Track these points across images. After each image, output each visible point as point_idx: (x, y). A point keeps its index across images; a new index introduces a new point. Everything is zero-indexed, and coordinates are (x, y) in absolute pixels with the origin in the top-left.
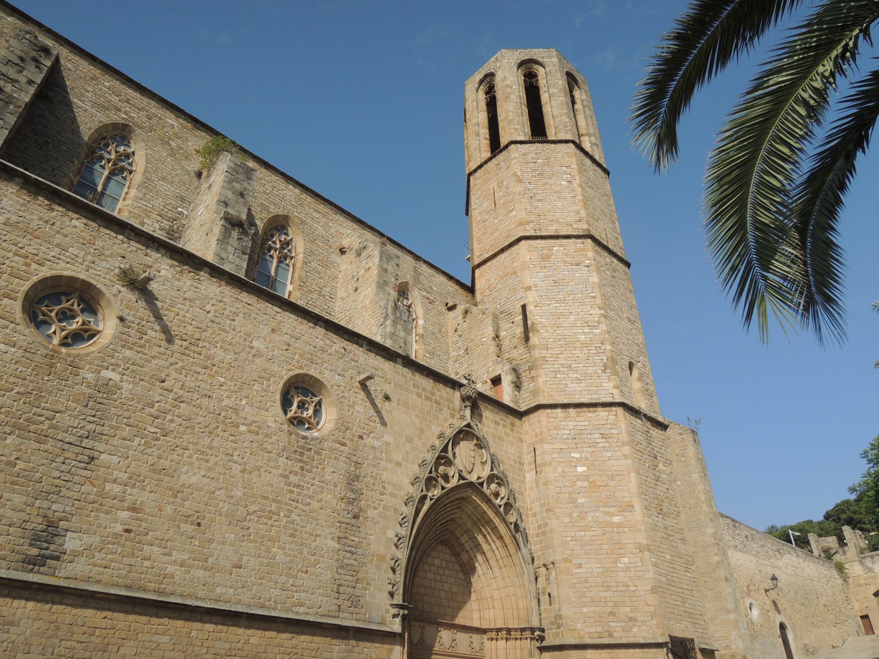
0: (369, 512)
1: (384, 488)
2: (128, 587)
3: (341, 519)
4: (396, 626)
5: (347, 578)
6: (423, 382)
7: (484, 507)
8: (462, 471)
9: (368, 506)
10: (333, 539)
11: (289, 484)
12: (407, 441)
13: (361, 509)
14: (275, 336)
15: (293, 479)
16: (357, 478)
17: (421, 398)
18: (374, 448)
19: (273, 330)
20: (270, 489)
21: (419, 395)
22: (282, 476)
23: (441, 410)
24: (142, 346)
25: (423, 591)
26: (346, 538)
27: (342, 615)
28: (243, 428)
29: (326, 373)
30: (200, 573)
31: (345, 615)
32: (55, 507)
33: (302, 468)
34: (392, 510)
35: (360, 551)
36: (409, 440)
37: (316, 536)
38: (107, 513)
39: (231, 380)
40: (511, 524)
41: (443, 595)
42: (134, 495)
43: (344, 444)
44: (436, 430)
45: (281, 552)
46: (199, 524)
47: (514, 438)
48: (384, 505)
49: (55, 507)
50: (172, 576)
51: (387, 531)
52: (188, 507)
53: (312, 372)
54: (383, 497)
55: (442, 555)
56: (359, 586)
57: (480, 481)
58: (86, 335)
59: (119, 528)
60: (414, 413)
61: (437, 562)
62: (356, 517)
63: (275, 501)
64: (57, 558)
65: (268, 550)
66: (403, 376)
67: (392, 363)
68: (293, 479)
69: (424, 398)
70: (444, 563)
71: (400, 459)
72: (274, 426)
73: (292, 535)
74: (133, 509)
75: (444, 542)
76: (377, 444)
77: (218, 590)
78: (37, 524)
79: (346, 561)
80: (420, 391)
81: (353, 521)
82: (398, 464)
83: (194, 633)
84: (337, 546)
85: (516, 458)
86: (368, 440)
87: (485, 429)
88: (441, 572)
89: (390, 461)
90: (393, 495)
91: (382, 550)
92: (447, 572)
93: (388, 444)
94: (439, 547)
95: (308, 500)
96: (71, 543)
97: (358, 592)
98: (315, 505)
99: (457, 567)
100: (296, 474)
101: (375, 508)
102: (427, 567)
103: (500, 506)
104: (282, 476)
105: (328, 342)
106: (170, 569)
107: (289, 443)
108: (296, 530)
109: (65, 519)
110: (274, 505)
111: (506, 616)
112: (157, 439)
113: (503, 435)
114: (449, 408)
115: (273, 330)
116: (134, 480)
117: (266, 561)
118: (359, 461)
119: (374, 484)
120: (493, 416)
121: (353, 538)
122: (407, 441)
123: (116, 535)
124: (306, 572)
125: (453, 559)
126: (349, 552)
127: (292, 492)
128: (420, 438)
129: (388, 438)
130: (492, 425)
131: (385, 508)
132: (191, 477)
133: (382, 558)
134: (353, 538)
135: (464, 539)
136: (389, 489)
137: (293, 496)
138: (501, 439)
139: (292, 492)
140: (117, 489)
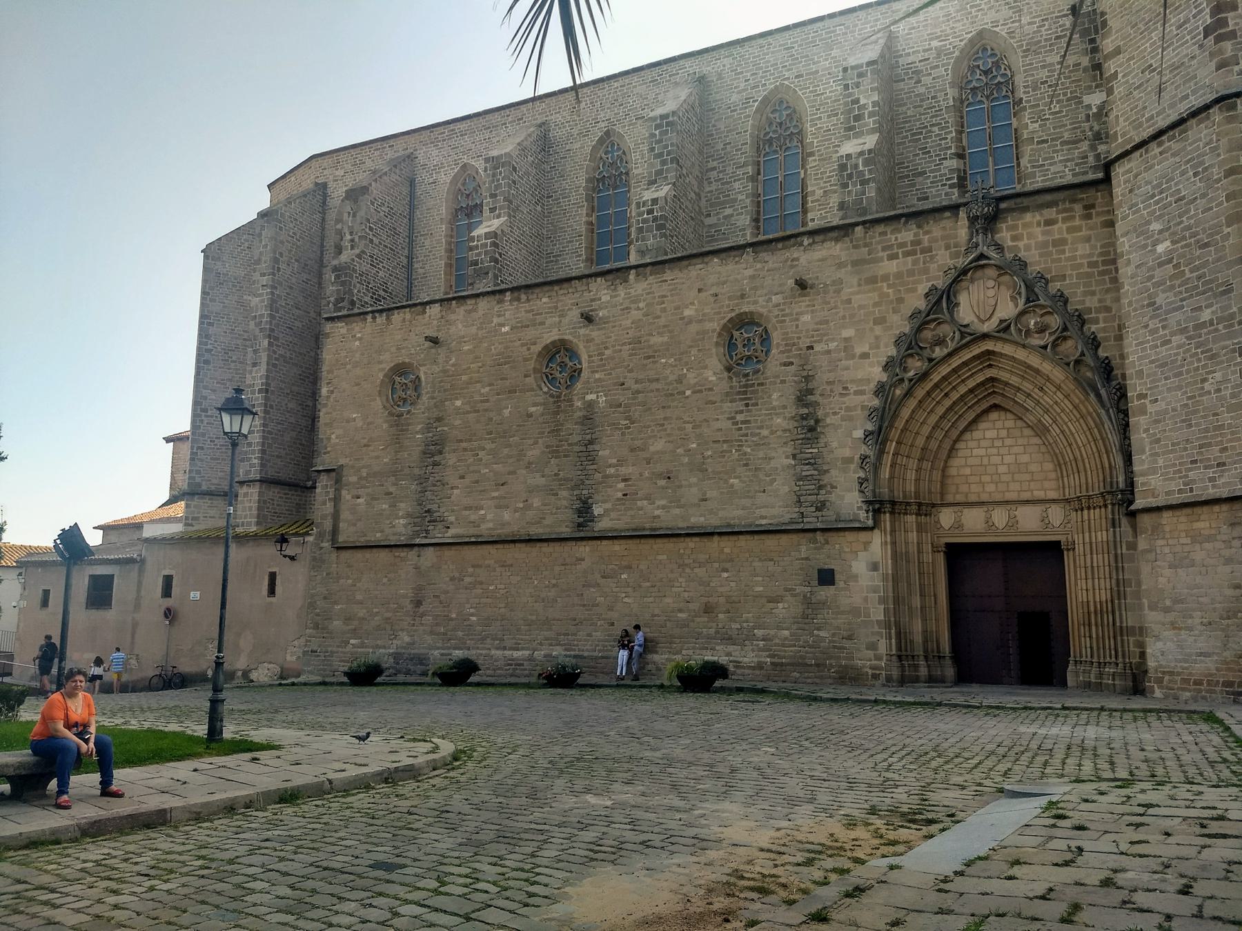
0: (828, 421)
1: (846, 388)
2: (634, 530)
3: (794, 438)
4: (870, 523)
5: (807, 487)
6: (899, 236)
7: (1021, 354)
8: (966, 326)
9: (827, 415)
10: (787, 457)
11: (736, 423)
12: (875, 324)
13: (817, 421)
14: (703, 295)
15: (739, 417)
16: (810, 392)
17: (898, 258)
18: (829, 352)
19: (700, 290)
20: (719, 433)
21: (892, 257)
22: (728, 419)
23: (932, 257)
24: (604, 365)
25: (968, 471)
26: (801, 453)
27: (805, 520)
28: (688, 393)
29: (761, 299)
30: (677, 511)
31: (808, 520)
32: (584, 492)
33: (747, 405)
34: (859, 408)
35: (819, 461)
36: (880, 321)
37: (770, 459)
38: (611, 487)
39: (672, 356)
40: (1068, 364)
41: (1002, 469)
42: (624, 471)
43: (792, 363)
44: (923, 288)
45: (736, 481)
46: (669, 478)
47: (1091, 229)
48: (847, 407)
49: (584, 492)
50: (659, 517)
51: (854, 432)
52: (660, 468)
53: (745, 309)
54: (845, 399)
55: (999, 424)
56: (823, 492)
57: (1004, 324)
58: (576, 374)
59: (620, 495)
60: (885, 284)
61: (989, 434)
62: (812, 429)
63: (724, 441)
64: (593, 521)
65: (726, 481)
66: (866, 245)
67: (847, 239)
68: (739, 417)
69: (900, 256)
70: (1004, 433)
71: (866, 349)
72: (714, 378)
73: (746, 465)
74: (625, 480)
75: (996, 407)
76: (832, 345)
77: (693, 520)
78: (578, 505)
79: (804, 473)
80: (895, 251)
81: (809, 435)
82: (865, 356)
83: (682, 551)
84: (793, 462)
85: (1095, 259)
86: (817, 348)
87: (1021, 244)
88: (998, 443)
89: (853, 357)
90: (862, 393)
91: (847, 453)
92: (1008, 442)
93: (847, 340)
94: (994, 415)
95: (758, 431)
96: (597, 510)
97: (821, 498)
98: (765, 432)
99: (1027, 432)
100: (741, 412)
101: (835, 414)
102: (971, 444)
103: (1045, 347)
104: (728, 419)
105: (759, 266)
106: (657, 512)
107: (731, 387)
108: (750, 459)
109: (591, 498)
110: (725, 445)
111: (1090, 480)
112: (629, 428)
113: (1065, 235)
114: (947, 247)
115: (700, 290)
116: (621, 462)
117: (725, 491)
118: (810, 373)
119: (832, 391)
120: (1041, 215)
121: (810, 451)
122: (875, 324)
123: (618, 499)
124: (764, 491)
125: (1019, 423)
126: (807, 464)
127: (740, 429)
128: (895, 311)
129: (848, 333)
130: (1038, 231)
131: (848, 409)
132: (658, 446)
133: (848, 461)
134: (810, 451)
135: (1020, 398)
136: (853, 388)
137: (743, 432)
138: (1063, 242)
139: (740, 429)
140: (612, 470)
